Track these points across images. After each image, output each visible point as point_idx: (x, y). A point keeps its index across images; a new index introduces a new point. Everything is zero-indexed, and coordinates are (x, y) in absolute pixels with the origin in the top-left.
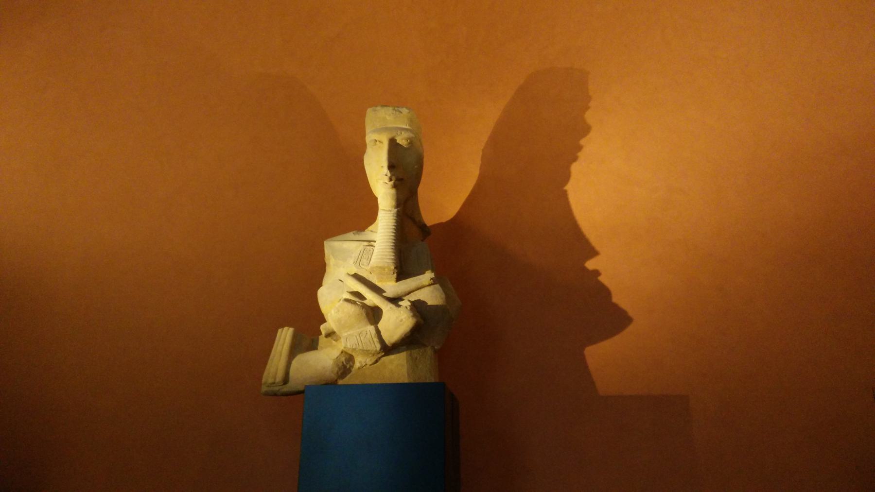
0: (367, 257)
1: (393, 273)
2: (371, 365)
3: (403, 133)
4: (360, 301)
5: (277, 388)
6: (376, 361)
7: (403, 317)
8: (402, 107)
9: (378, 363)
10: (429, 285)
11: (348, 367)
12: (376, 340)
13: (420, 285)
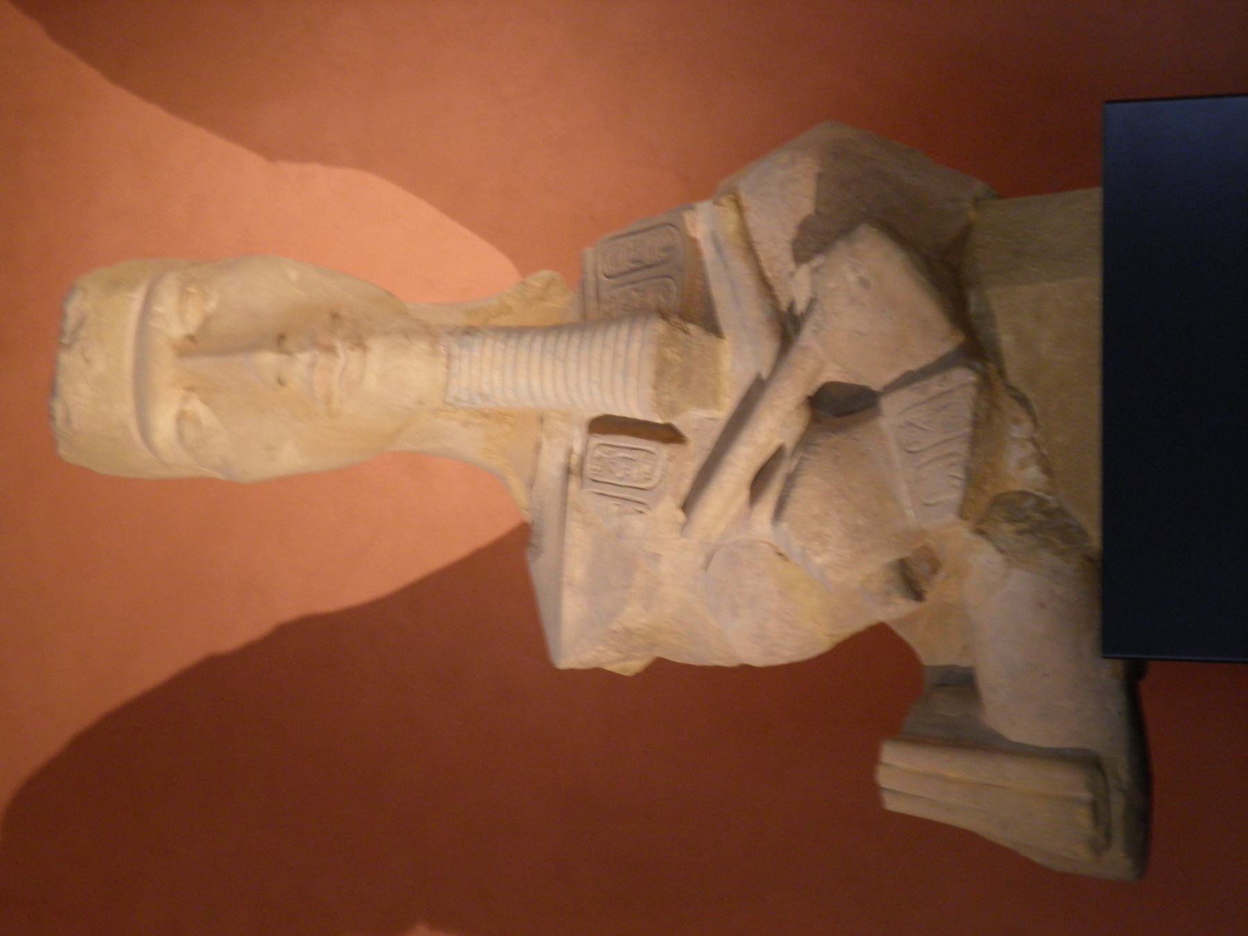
1: (686, 332)
2: (1035, 421)
5: (1118, 806)
6: (1023, 401)
7: (852, 278)
9: (1030, 395)
10: (740, 209)
11: (1038, 516)
12: (935, 385)
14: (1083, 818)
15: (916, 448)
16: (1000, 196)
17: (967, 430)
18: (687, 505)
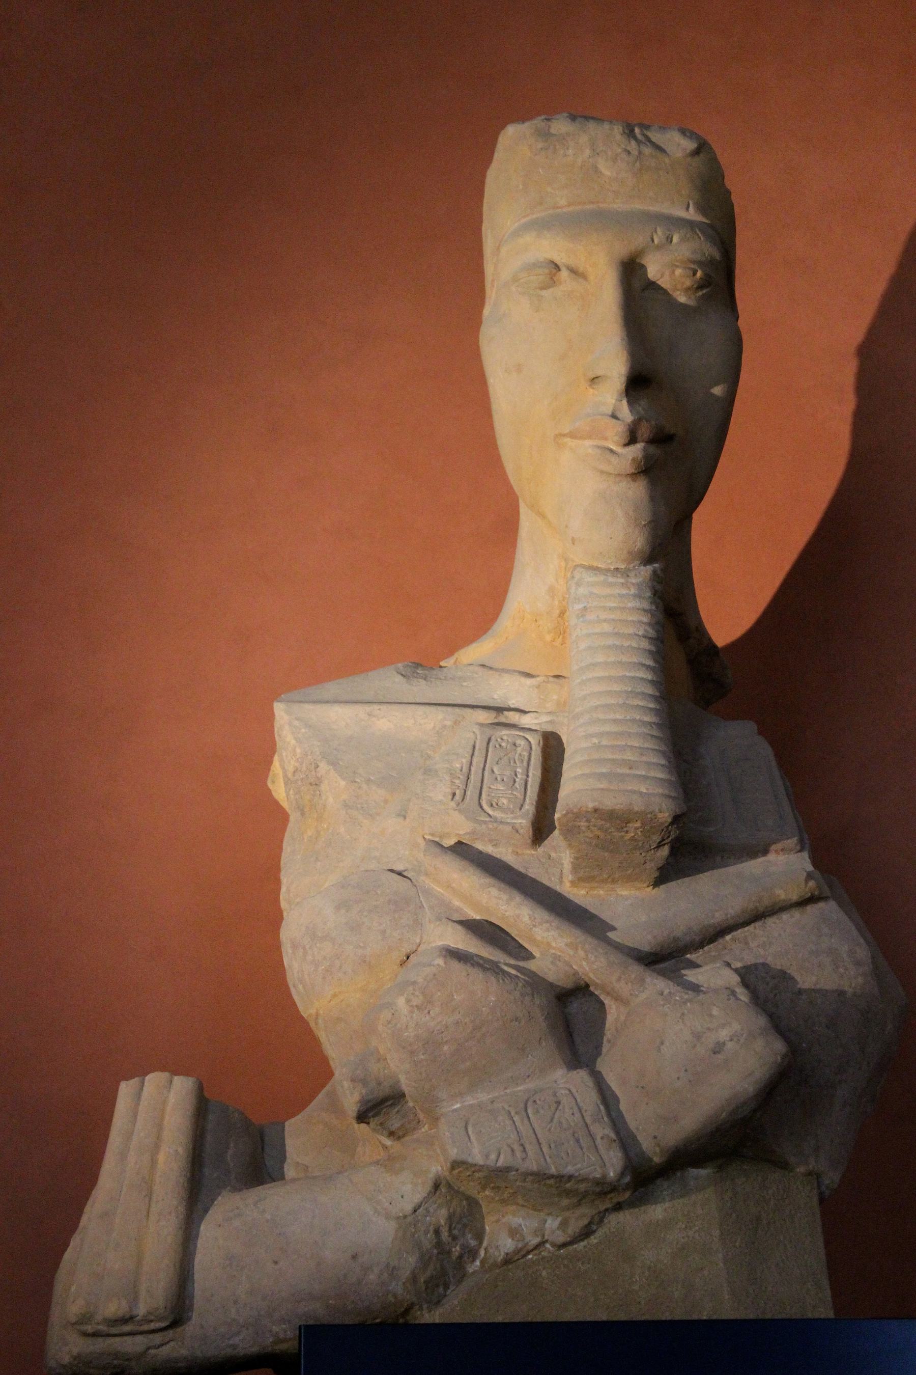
0: (508, 773)
1: (660, 845)
2: (564, 1245)
3: (675, 239)
4: (513, 962)
5: (132, 1345)
6: (586, 1233)
7: (724, 1034)
8: (663, 128)
9: (593, 1240)
10: (803, 903)
11: (456, 1250)
12: (603, 1131)
13: (766, 902)
14: (113, 1308)
15: (530, 1111)
16: (822, 1200)
17: (553, 1170)
18: (461, 850)
